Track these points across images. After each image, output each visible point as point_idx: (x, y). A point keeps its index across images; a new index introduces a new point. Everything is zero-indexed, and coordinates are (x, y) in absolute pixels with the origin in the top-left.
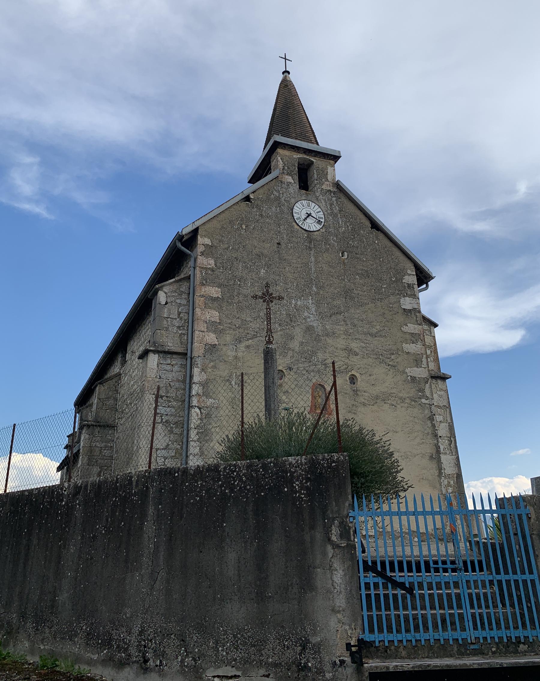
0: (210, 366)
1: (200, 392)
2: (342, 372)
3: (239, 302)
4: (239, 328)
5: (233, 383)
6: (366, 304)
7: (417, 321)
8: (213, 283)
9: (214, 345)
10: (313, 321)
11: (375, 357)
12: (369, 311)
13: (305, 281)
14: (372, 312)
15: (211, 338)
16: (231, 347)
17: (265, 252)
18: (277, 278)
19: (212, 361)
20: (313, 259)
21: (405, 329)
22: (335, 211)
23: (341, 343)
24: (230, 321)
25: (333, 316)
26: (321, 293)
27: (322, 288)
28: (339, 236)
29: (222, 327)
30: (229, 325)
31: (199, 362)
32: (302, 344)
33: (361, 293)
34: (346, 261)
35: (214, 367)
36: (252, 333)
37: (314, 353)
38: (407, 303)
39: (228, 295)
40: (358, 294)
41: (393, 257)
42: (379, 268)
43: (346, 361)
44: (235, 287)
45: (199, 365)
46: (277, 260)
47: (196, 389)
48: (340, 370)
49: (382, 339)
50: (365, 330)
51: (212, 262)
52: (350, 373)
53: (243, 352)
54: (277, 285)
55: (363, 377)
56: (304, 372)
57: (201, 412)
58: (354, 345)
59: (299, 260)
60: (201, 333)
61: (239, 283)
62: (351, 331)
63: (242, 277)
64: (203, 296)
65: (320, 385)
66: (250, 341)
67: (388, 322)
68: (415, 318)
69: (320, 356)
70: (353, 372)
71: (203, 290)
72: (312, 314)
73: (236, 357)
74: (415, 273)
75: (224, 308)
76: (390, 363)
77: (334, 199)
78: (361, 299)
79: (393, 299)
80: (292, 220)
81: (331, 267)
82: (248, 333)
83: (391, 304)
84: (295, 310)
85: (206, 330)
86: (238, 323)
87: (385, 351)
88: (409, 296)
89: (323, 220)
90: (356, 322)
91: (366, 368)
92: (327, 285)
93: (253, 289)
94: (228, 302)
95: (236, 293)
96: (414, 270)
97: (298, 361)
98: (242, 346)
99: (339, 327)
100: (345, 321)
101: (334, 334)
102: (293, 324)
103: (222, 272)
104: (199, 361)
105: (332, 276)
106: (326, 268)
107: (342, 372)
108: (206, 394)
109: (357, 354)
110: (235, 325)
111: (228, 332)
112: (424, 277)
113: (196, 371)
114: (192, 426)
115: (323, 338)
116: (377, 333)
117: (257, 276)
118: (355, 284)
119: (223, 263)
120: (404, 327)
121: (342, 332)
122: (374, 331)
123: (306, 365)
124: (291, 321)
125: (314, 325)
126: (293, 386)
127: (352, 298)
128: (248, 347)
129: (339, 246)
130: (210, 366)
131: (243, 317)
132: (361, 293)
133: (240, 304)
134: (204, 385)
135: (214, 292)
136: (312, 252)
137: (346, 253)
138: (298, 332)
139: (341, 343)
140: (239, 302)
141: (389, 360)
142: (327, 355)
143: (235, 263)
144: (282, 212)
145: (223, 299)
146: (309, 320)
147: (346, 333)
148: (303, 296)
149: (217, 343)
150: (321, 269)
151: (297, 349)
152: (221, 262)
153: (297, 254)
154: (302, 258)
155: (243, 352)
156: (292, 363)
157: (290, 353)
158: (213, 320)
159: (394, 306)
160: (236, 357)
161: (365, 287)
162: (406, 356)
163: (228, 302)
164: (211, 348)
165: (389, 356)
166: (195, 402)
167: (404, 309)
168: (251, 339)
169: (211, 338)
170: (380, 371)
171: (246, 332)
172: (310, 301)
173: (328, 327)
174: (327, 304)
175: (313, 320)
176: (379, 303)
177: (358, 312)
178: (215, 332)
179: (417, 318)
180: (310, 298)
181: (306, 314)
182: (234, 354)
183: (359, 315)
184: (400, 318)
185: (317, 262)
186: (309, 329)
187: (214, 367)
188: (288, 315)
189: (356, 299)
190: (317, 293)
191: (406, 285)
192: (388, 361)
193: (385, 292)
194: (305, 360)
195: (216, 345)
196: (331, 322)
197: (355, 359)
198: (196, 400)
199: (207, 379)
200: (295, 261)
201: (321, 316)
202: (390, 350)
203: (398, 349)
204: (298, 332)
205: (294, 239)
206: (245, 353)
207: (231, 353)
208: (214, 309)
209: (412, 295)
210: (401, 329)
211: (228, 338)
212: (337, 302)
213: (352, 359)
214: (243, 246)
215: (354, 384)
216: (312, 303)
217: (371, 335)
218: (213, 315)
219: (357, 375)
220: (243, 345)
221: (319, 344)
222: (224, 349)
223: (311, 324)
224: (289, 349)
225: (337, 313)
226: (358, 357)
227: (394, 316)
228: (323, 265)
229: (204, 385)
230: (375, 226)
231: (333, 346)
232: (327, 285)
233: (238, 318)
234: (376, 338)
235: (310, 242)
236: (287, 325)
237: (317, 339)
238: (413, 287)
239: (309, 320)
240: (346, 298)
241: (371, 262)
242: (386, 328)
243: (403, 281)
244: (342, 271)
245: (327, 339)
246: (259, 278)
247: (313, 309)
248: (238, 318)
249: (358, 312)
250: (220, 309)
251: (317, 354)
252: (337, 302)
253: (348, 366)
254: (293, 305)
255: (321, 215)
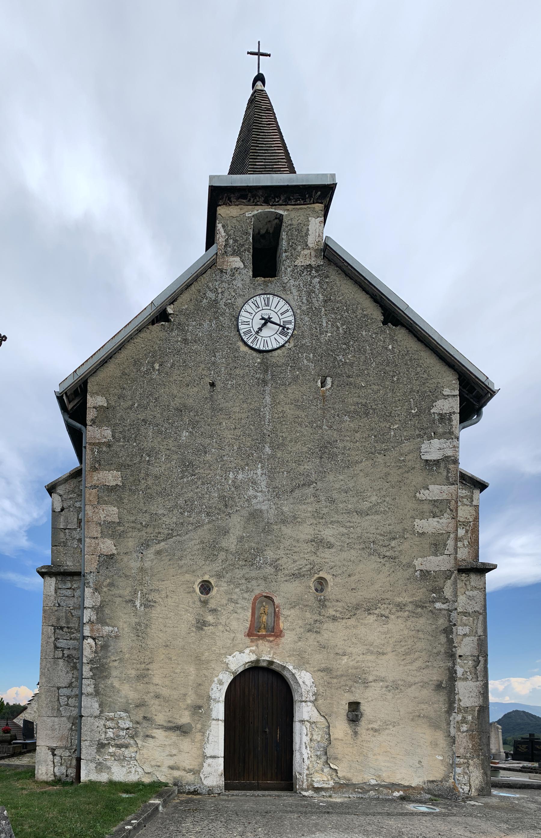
0: (105, 583)
1: (94, 618)
2: (304, 576)
3: (148, 487)
4: (146, 526)
5: (138, 603)
6: (357, 462)
7: (447, 478)
8: (109, 465)
9: (111, 555)
10: (261, 501)
11: (362, 546)
12: (361, 474)
13: (253, 440)
14: (367, 475)
15: (108, 546)
16: (135, 555)
17: (190, 402)
18: (208, 441)
19: (109, 577)
20: (268, 399)
21: (424, 495)
22: (316, 305)
23: (306, 531)
24: (133, 518)
25: (297, 491)
26: (279, 455)
27: (281, 446)
28: (319, 350)
29: (122, 528)
30: (133, 525)
31: (91, 580)
32: (241, 539)
33: (348, 445)
34: (328, 393)
35: (111, 585)
36: (166, 532)
37: (260, 551)
38: (433, 449)
39: (131, 479)
40: (345, 447)
41: (419, 369)
42: (390, 394)
43: (312, 558)
44: (142, 465)
45: (91, 584)
46: (209, 412)
47: (88, 615)
48: (299, 573)
49: (377, 517)
50: (350, 506)
51: (108, 433)
52: (316, 576)
53: (152, 561)
54: (206, 453)
55: (338, 580)
56: (243, 581)
57: (96, 643)
58: (328, 533)
59: (245, 406)
60: (93, 540)
61: (147, 458)
62: (325, 510)
63: (153, 448)
64: (95, 487)
65: (266, 597)
66: (163, 544)
67: (393, 487)
68: (445, 474)
69: (270, 554)
70: (321, 574)
71: (96, 478)
72: (261, 491)
73: (142, 570)
74: (457, 392)
75: (125, 501)
76: (388, 554)
77: (317, 280)
78: (349, 455)
79: (407, 446)
80: (237, 338)
81: (298, 407)
82: (159, 533)
83: (401, 455)
84: (233, 489)
85: (99, 536)
86: (145, 519)
87: (381, 535)
88: (440, 436)
89: (291, 326)
90: (335, 495)
91: (344, 565)
92: (291, 441)
93: (169, 465)
94: (130, 490)
95: (142, 475)
96: (457, 386)
97: (233, 565)
98: (150, 553)
99: (304, 507)
100: (315, 496)
101: (295, 518)
102: (229, 510)
103: (123, 446)
104: (91, 579)
105: (300, 424)
106: (290, 411)
107: (304, 576)
108: (101, 621)
109: (330, 546)
110: (141, 523)
111: (130, 534)
112: (474, 395)
113: (88, 591)
114: (85, 661)
115: (275, 527)
116: (370, 508)
117: (176, 443)
118: (339, 430)
119: (124, 431)
120: (422, 491)
121: (309, 515)
122: (366, 505)
123: (246, 570)
124: (226, 506)
125: (264, 508)
126: (224, 602)
127: (333, 457)
128: (159, 553)
129: (318, 369)
130: (105, 583)
131: (153, 509)
132: (348, 445)
133: (148, 491)
134: (99, 609)
135: (111, 477)
136: (268, 388)
137: (329, 380)
138: (236, 523)
139: (306, 531)
140: (148, 487)
141: (385, 549)
142: (281, 552)
143: (142, 428)
144: (221, 327)
145: (124, 485)
146: (254, 501)
147: (317, 515)
148: (247, 465)
149: (115, 552)
150: (281, 415)
151: (233, 548)
152: (121, 430)
153: (242, 397)
154: (249, 401)
155: (152, 561)
156: (224, 569)
157: (222, 555)
158: (109, 519)
159: (409, 457)
160: (142, 570)
161: (358, 435)
162: (417, 539)
163: (130, 490)
164: (108, 560)
165: (387, 543)
166: (87, 632)
167: (427, 460)
168: (163, 540)
169: (108, 546)
170: (368, 567)
171: (157, 531)
172: (259, 472)
173: (285, 509)
174: (288, 472)
175: (261, 500)
176: (380, 459)
177: (341, 477)
178: (112, 536)
179: (448, 472)
180: (259, 466)
181: (251, 492)
182: (138, 564)
183: (342, 483)
184: (416, 478)
185: (275, 403)
186: (255, 515)
187: (111, 585)
188: (222, 498)
189: (340, 457)
190: (273, 457)
191: (437, 417)
192: (383, 551)
193: (395, 436)
194: (244, 563)
195: (113, 555)
196: (291, 500)
197: (326, 554)
198: (88, 629)
199: (102, 602)
200: (237, 409)
201: (276, 493)
202: (390, 533)
203: (404, 530)
204: (236, 523)
205: (237, 371)
206: (155, 562)
207: (135, 565)
208: (112, 504)
209: (445, 433)
210: (415, 496)
211: (131, 543)
212: (307, 466)
213: (322, 555)
214: (156, 399)
215: (322, 590)
216: (262, 474)
217: (360, 513)
218: (110, 512)
219: (328, 577)
220: (152, 550)
221: (270, 537)
222: (125, 559)
223: (259, 507)
224: (222, 549)
225: (304, 485)
226: (333, 550)
227: (406, 475)
228: (287, 408)
229: (99, 609)
230: (394, 316)
231: (291, 537)
232: (291, 441)
233: (146, 512)
234: (367, 518)
235: (266, 371)
236: (218, 514)
237: (267, 530)
238: (450, 420)
239: (254, 501)
240: (321, 458)
241: (375, 388)
242: (387, 499)
243: (432, 411)
244: (319, 412)
245: (283, 528)
246: (179, 447)
247: (264, 484)
248: (146, 512)
249: (341, 477)
250: (119, 502)
251: (265, 553)
252: (307, 466)
253: (314, 566)
254: (230, 481)
255: (289, 317)
